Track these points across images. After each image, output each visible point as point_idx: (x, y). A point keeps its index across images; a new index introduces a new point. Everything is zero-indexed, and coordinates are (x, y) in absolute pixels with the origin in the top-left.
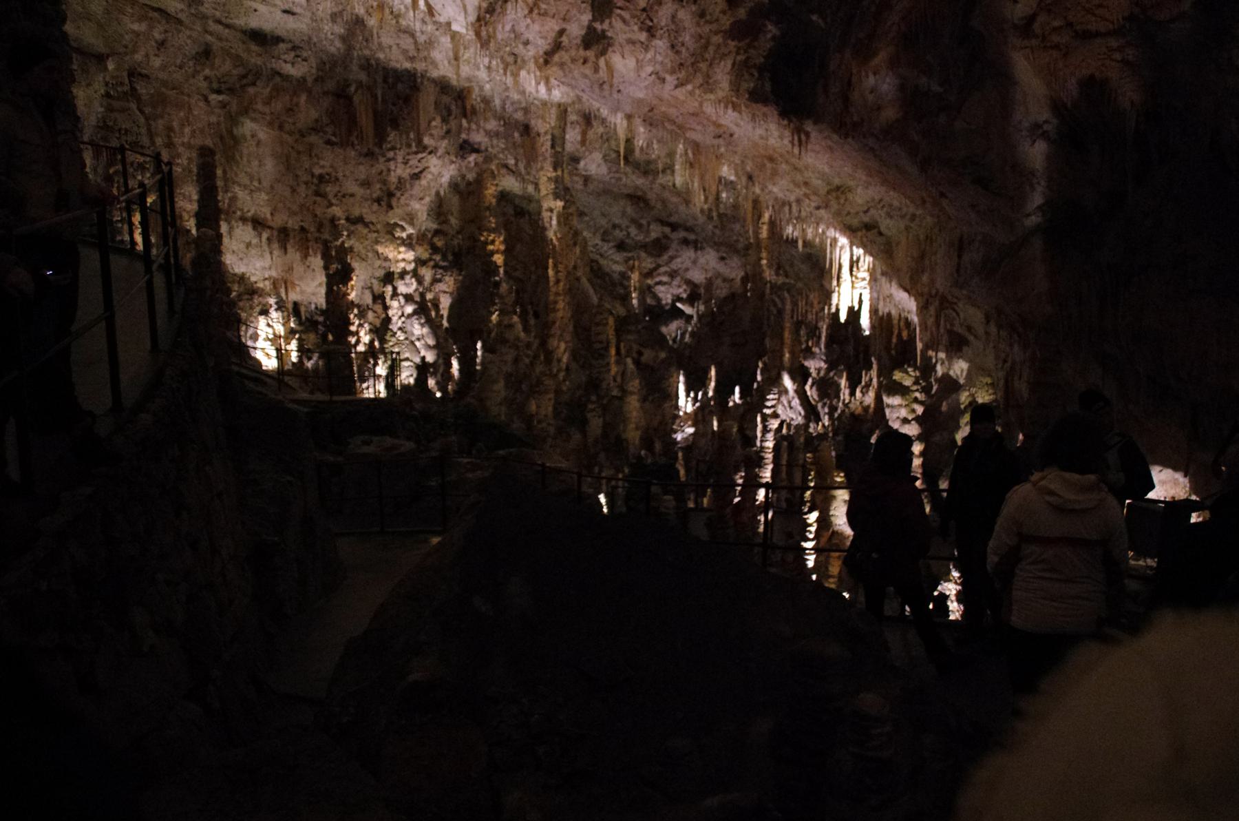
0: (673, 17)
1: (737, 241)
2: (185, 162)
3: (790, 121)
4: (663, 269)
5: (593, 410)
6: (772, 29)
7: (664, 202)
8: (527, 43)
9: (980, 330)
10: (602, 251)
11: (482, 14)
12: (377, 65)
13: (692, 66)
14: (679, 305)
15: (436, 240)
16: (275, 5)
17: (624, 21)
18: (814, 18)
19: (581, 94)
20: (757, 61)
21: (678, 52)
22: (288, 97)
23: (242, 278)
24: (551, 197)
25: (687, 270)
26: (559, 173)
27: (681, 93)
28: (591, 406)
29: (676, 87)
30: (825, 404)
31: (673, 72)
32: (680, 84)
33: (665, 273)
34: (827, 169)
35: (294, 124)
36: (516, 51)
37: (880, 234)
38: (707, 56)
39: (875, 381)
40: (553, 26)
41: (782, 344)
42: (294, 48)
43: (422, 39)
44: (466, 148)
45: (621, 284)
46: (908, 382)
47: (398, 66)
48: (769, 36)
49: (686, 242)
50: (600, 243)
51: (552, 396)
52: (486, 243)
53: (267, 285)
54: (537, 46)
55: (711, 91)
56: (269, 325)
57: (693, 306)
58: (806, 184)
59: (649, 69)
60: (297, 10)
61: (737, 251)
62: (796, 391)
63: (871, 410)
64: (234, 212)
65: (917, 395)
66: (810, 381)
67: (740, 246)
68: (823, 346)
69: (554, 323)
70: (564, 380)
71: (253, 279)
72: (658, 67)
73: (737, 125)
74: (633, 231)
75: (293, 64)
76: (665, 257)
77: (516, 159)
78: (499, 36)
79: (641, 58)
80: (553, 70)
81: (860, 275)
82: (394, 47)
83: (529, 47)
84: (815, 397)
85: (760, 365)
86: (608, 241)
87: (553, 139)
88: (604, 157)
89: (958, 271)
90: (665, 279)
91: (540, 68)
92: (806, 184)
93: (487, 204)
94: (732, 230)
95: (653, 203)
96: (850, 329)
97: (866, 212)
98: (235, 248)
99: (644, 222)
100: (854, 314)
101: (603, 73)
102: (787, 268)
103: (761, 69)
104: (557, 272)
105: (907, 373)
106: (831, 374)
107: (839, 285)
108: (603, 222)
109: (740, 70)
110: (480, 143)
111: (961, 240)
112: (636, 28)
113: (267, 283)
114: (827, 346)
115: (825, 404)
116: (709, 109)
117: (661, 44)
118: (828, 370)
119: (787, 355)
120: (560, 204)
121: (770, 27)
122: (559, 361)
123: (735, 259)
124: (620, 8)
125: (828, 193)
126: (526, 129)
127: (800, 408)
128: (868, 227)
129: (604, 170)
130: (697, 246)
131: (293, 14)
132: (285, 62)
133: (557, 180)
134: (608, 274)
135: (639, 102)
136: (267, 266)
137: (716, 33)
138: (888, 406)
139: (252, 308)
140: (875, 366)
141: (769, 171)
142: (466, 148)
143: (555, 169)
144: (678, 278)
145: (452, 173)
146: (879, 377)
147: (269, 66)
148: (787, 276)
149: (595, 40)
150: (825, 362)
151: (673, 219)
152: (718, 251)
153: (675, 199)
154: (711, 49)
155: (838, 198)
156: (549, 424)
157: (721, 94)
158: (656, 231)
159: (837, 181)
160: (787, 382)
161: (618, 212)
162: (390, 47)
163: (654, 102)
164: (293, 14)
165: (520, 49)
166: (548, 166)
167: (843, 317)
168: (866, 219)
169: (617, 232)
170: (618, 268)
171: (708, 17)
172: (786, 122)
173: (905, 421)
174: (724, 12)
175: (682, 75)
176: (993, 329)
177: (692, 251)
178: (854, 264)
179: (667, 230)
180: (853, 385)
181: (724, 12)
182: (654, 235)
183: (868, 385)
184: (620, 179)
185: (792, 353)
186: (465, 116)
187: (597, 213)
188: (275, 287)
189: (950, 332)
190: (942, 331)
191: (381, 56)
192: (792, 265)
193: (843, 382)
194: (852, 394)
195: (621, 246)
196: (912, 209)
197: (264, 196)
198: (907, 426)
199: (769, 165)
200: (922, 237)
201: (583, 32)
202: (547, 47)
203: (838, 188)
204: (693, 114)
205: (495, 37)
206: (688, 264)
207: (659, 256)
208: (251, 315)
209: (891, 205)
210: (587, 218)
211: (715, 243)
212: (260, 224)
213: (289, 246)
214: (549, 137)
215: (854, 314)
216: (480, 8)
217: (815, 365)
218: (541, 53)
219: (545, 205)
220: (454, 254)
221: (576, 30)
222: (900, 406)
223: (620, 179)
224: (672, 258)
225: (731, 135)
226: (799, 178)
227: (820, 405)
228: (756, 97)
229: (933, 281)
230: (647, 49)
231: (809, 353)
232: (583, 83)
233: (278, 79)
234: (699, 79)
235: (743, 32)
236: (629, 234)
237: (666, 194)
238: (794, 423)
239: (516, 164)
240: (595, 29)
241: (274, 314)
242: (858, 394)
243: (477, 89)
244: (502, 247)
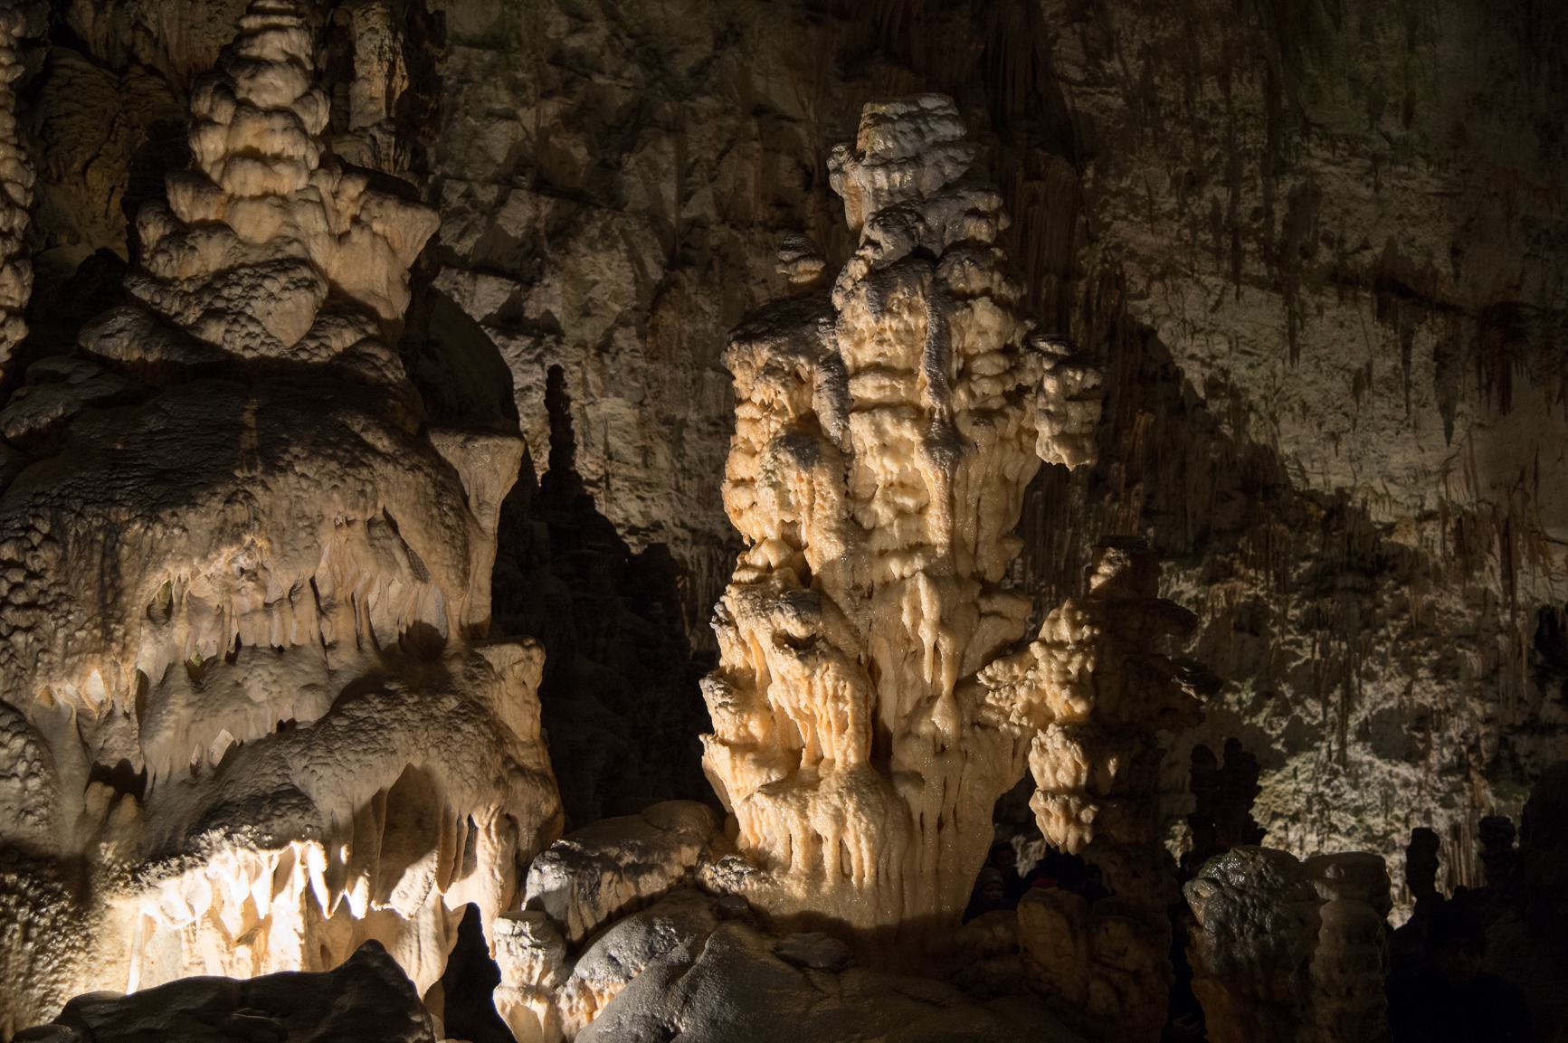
2: (1135, 67)
23: (1337, 508)
53: (1435, 540)
56: (804, 439)
64: (1307, 253)
71: (1380, 514)
98: (1312, 397)
113: (1432, 530)
136: (1432, 461)
139: (1370, 622)
188: (1463, 549)
197: (1424, 178)
208: (1367, 651)
212: (1404, 292)
213: (1519, 381)
241: (864, 329)
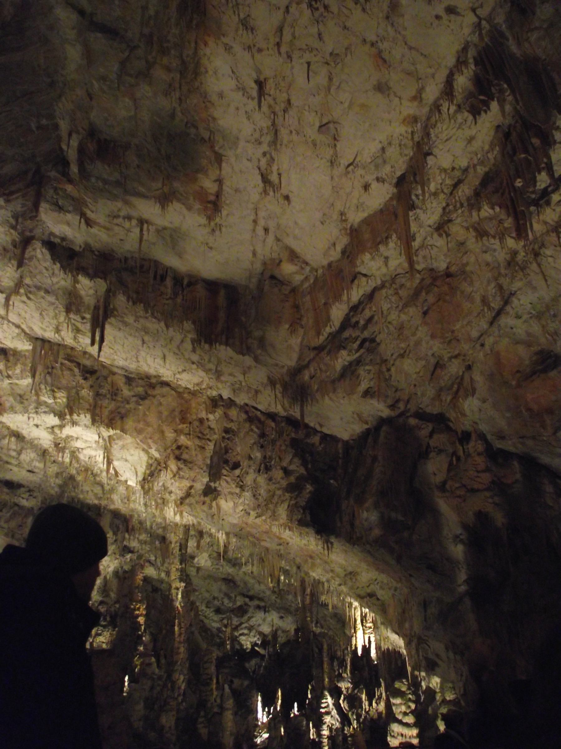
0: (254, 481)
1: (290, 606)
3: (322, 536)
4: (244, 626)
6: (309, 488)
7: (245, 583)
8: (171, 492)
9: (443, 654)
10: (206, 614)
11: (146, 476)
12: (78, 501)
13: (264, 506)
14: (256, 648)
15: (100, 607)
16: (23, 468)
17: (227, 482)
18: (332, 481)
19: (200, 521)
20: (302, 505)
21: (257, 499)
22: (20, 519)
24: (178, 580)
25: (259, 625)
26: (184, 566)
27: (258, 521)
29: (256, 517)
31: (254, 510)
32: (259, 516)
33: (246, 627)
34: (344, 562)
35: (22, 535)
36: (164, 497)
37: (378, 599)
38: (273, 501)
39: (384, 695)
40: (186, 484)
41: (323, 672)
42: (30, 491)
43: (107, 488)
44: (126, 550)
45: (218, 636)
46: (404, 689)
47: (91, 502)
48: (308, 491)
49: (258, 607)
50: (205, 609)
52: (135, 610)
54: (176, 494)
55: (276, 520)
57: (265, 649)
58: (332, 571)
59: (241, 508)
60: (36, 470)
62: (334, 704)
63: (384, 715)
65: (410, 696)
72: (246, 507)
73: (291, 538)
74: (226, 601)
75: (27, 500)
76: (246, 618)
77: (156, 557)
78: (155, 489)
79: (236, 501)
80: (186, 508)
81: (368, 625)
82: (90, 492)
83: (172, 495)
84: (347, 708)
85: (310, 687)
86: (209, 608)
87: (181, 545)
88: (210, 555)
89: (425, 620)
90: (246, 631)
91: (177, 507)
92: (332, 571)
93: (137, 585)
94: (287, 599)
96: (365, 659)
97: (368, 587)
99: (233, 595)
100: (366, 650)
101: (215, 509)
102: (322, 622)
103: (304, 509)
105: (403, 683)
106: (356, 691)
107: (355, 632)
108: (207, 595)
109: (291, 510)
110: (134, 547)
111: (425, 602)
112: (234, 486)
115: (353, 713)
116: (275, 529)
117: (247, 494)
118: (354, 689)
119: (327, 680)
120: (183, 584)
121: (308, 486)
123: (290, 618)
124: (225, 476)
125: (346, 575)
126: (163, 539)
127: (337, 716)
128: (371, 595)
129: (209, 563)
130: (265, 609)
131: (33, 472)
132: (23, 498)
134: (209, 629)
135: (234, 525)
137: (279, 489)
138: (394, 704)
140: (383, 685)
141: (310, 565)
142: (126, 550)
143: (181, 564)
144: (254, 631)
145: (115, 565)
146: (386, 692)
147: (12, 501)
148: (322, 627)
149: (210, 492)
150: (351, 683)
151: (251, 593)
152: (279, 613)
153: (252, 581)
154: (276, 498)
155: (351, 579)
157: (281, 521)
158: (240, 601)
159: (350, 569)
161: (217, 589)
162: (88, 491)
163: (244, 525)
164: (33, 472)
165: (167, 496)
166: (177, 561)
167: (360, 652)
168: (369, 591)
169: (216, 602)
170: (216, 625)
171: (274, 481)
172: (319, 537)
173: (405, 714)
174: (282, 478)
175: (259, 511)
176: (451, 655)
177: (263, 613)
178: (364, 618)
179: (247, 600)
180: (370, 698)
181: (282, 478)
182: (238, 604)
183: (380, 698)
184: (219, 569)
185: (330, 679)
186: (127, 531)
187: (203, 590)
189: (426, 659)
190: (421, 658)
191: (81, 496)
192: (325, 621)
193: (364, 697)
194: (370, 704)
195: (218, 611)
196: (395, 584)
198: (407, 717)
199: (310, 560)
200: (402, 601)
201: (203, 487)
202: (183, 495)
203: (351, 573)
204: (265, 532)
205: (153, 489)
206: (260, 622)
207: (242, 616)
209: (382, 582)
210: (197, 593)
211: (277, 608)
214: (178, 544)
215: (366, 650)
216: (145, 473)
217: (345, 686)
218: (179, 498)
219: (174, 586)
220: (111, 617)
221: (199, 486)
222: (401, 704)
223: (219, 569)
224: (250, 618)
225: (288, 544)
226: (327, 567)
227: (350, 714)
228: (302, 523)
229: (411, 627)
230: (240, 497)
231: (340, 678)
232: (202, 515)
233: (16, 508)
234: (269, 513)
235: (294, 488)
236: (223, 603)
237: (247, 578)
238: (334, 727)
239: (156, 560)
240: (210, 486)
242: (374, 704)
243: (136, 516)
244: (144, 612)
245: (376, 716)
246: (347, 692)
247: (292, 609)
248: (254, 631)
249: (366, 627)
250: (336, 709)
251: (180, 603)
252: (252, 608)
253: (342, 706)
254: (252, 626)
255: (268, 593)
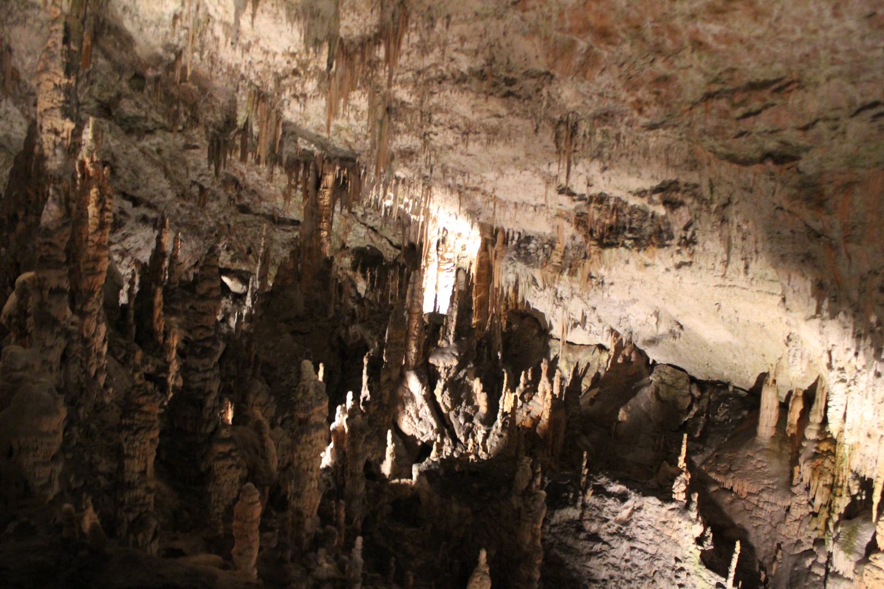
4: (113, 248)
5: (226, 456)
7: (136, 172)
25: (139, 249)
28: (222, 448)
30: (458, 413)
41: (407, 335)
49: (144, 220)
51: (155, 434)
61: (199, 235)
66: (440, 385)
67: (204, 228)
68: (451, 338)
69: (91, 293)
70: (106, 386)
76: (119, 235)
85: (365, 361)
95: (119, 172)
104: (102, 211)
106: (461, 374)
114: (456, 339)
115: (458, 413)
118: (459, 368)
122: (99, 355)
123: (193, 243)
127: (431, 420)
133: (68, 91)
144: (129, 258)
151: (138, 193)
156: (148, 490)
160: (414, 384)
179: (127, 205)
217: (444, 363)
224: (125, 236)
227: (452, 414)
245: (528, 423)
246: (448, 373)
247: (204, 228)
248: (129, 258)
249: (443, 258)
250: (429, 406)
251: (90, 153)
252: (133, 220)
253: (439, 399)
254: (127, 251)
255: (170, 195)
